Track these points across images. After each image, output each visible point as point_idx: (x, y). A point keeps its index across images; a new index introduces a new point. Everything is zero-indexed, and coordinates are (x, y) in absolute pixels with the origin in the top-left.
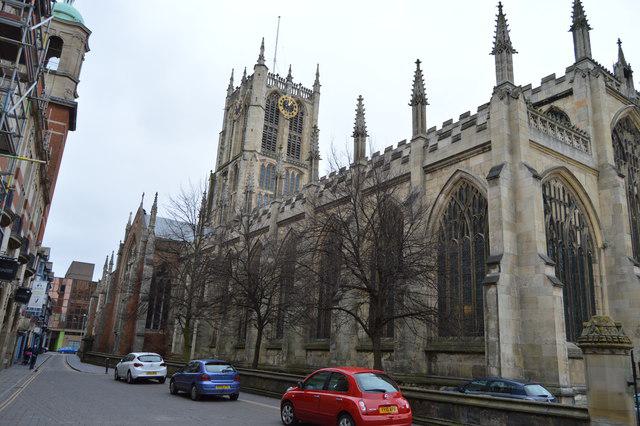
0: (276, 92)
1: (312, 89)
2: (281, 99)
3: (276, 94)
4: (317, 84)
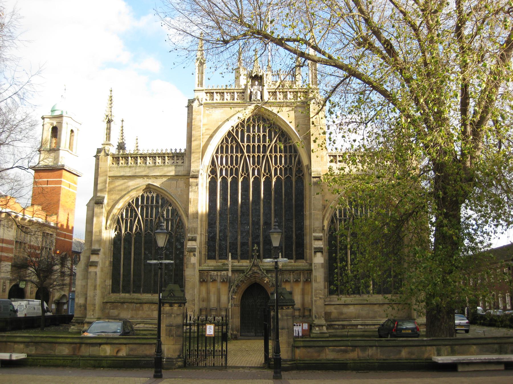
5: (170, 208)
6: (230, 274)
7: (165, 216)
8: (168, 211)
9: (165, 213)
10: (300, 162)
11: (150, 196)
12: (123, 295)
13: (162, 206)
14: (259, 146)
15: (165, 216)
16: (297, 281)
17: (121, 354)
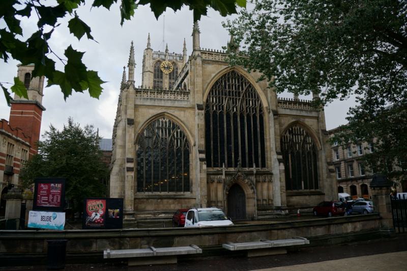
0: (159, 61)
1: (182, 53)
3: (159, 62)
5: (179, 131)
6: (223, 177)
7: (175, 136)
8: (177, 133)
9: (175, 134)
10: (261, 105)
11: (164, 121)
12: (147, 193)
13: (173, 129)
15: (175, 136)
16: (265, 181)
17: (357, 230)
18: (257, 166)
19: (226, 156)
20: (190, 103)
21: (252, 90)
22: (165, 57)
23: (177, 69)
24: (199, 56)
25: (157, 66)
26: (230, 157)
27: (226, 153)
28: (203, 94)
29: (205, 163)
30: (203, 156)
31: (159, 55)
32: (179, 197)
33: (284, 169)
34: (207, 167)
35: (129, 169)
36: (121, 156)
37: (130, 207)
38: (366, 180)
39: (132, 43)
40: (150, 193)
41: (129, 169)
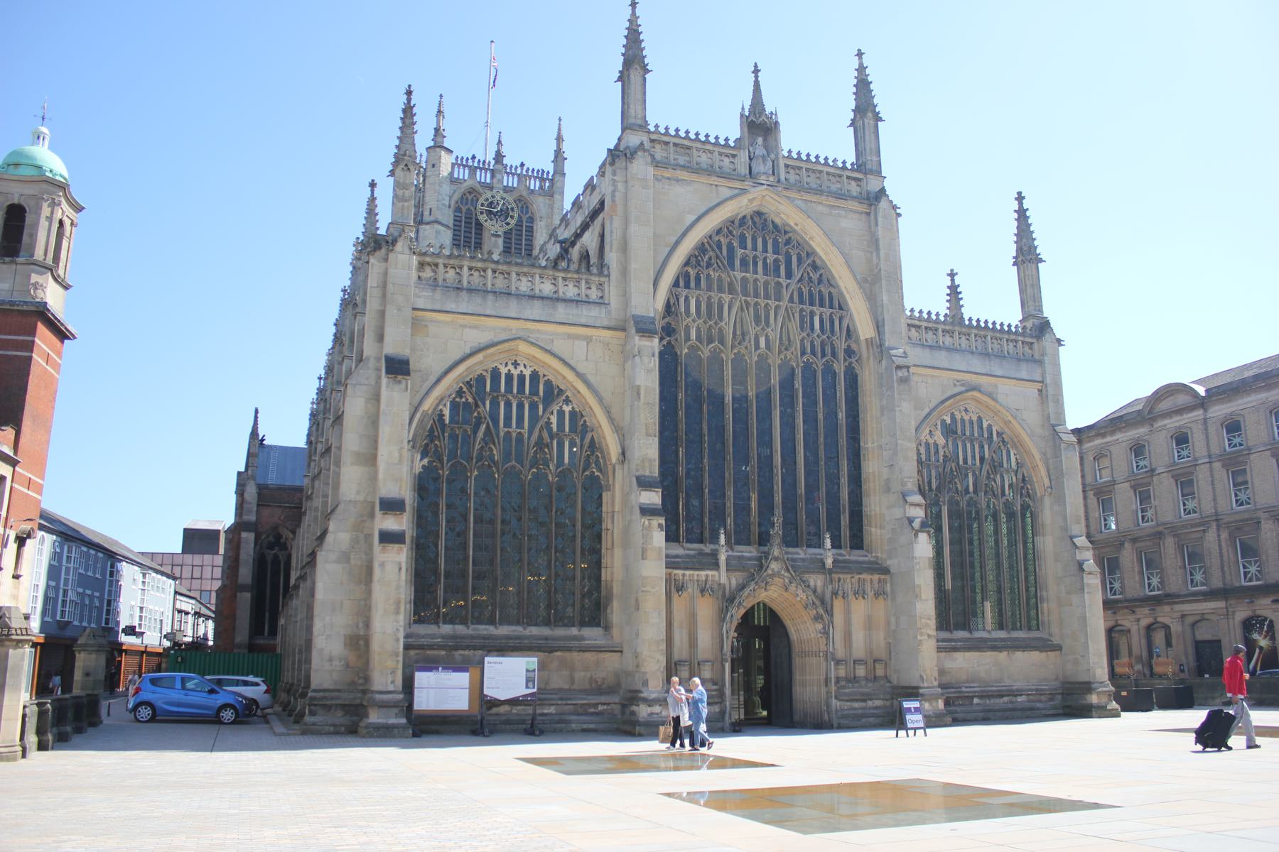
0: (472, 191)
2: (481, 200)
4: (559, 157)
5: (567, 409)
8: (561, 413)
9: (554, 419)
11: (515, 372)
12: (446, 629)
14: (766, 284)
18: (836, 544)
19: (730, 504)
20: (609, 313)
21: (820, 281)
22: (493, 177)
23: (531, 220)
24: (645, 151)
25: (464, 209)
26: (742, 509)
27: (730, 493)
28: (656, 283)
29: (660, 526)
30: (653, 498)
31: (473, 170)
32: (561, 643)
33: (932, 556)
34: (668, 539)
35: (388, 538)
36: (358, 493)
37: (390, 679)
38: (1167, 608)
39: (409, 93)
40: (460, 629)
41: (388, 538)
